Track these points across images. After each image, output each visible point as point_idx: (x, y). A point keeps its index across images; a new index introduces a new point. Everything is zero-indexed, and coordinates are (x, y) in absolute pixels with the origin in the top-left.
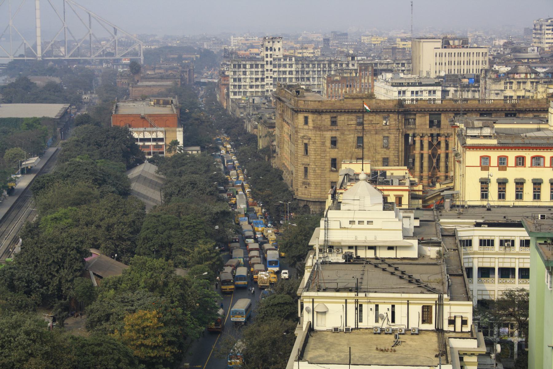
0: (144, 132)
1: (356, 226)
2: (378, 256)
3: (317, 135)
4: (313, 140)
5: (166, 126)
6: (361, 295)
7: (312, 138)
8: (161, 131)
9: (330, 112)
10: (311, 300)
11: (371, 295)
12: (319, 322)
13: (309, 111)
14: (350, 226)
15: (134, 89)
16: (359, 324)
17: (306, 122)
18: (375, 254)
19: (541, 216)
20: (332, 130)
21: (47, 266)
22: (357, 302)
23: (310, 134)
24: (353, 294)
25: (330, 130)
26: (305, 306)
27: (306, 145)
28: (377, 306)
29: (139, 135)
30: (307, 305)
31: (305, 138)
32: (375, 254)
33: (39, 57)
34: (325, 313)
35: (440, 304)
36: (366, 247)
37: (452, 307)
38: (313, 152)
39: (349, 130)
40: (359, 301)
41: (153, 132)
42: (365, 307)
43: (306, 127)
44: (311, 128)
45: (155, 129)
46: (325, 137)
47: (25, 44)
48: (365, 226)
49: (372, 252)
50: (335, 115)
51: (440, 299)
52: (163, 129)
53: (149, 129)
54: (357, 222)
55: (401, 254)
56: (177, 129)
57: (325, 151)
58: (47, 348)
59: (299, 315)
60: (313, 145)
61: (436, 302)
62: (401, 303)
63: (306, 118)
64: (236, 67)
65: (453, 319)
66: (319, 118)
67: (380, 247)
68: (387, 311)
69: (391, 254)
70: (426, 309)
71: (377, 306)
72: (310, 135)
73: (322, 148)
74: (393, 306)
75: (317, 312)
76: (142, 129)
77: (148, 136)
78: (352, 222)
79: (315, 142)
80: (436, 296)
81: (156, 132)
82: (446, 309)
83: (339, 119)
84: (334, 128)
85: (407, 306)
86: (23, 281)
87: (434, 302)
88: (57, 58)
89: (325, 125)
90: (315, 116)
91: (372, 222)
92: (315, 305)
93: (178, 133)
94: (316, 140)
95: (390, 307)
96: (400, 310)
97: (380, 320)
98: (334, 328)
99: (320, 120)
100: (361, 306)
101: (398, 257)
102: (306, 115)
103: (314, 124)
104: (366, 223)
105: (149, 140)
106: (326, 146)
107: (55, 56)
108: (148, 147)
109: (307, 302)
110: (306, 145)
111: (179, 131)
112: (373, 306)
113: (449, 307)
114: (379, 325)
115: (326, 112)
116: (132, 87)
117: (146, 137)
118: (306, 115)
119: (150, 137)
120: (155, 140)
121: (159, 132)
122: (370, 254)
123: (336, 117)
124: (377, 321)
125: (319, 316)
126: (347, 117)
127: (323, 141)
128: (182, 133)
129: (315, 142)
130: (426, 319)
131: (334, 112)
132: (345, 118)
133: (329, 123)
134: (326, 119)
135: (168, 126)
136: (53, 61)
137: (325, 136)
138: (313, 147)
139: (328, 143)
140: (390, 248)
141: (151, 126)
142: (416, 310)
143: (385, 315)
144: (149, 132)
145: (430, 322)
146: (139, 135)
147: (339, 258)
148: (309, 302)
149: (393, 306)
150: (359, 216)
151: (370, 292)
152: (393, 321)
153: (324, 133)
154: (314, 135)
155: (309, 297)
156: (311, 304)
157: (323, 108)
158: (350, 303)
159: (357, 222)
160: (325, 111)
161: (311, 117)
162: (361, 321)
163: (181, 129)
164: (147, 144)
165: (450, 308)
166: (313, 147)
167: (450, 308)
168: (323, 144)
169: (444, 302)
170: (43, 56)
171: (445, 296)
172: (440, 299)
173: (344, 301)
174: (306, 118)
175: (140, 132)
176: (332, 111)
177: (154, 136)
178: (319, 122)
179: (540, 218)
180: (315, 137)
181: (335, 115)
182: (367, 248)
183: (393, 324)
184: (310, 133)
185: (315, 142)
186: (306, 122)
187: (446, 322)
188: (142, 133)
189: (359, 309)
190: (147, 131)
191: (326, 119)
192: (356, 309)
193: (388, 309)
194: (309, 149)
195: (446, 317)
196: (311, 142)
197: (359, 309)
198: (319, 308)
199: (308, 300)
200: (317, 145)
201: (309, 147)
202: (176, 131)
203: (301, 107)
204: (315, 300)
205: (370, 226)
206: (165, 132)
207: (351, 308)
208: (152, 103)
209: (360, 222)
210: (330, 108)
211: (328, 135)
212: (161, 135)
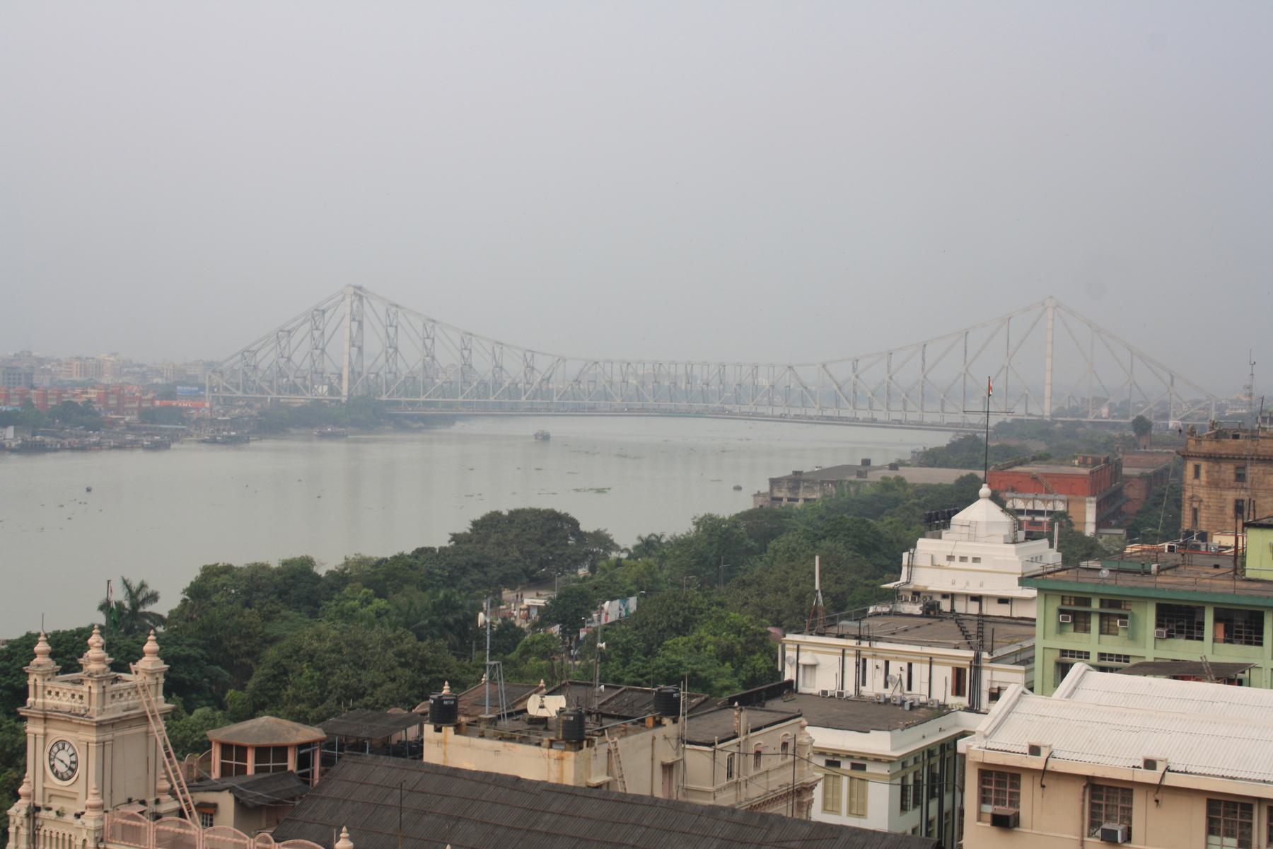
0: (1034, 499)
1: (956, 564)
2: (984, 612)
3: (1211, 496)
4: (1206, 504)
5: (1070, 493)
6: (865, 644)
7: (1204, 500)
8: (1061, 500)
9: (1234, 458)
10: (796, 647)
11: (880, 645)
12: (808, 681)
13: (1200, 457)
14: (946, 563)
15: (1125, 457)
16: (861, 688)
17: (1197, 475)
18: (980, 608)
19: (1169, 547)
20: (1235, 488)
21: (660, 631)
22: (858, 654)
23: (1202, 493)
24: (853, 643)
25: (1233, 488)
26: (788, 654)
27: (1195, 511)
28: (887, 663)
29: (1026, 505)
30: (790, 654)
31: (1195, 499)
32: (980, 608)
33: (1048, 417)
34: (814, 666)
35: (976, 665)
36: (966, 595)
37: (994, 672)
38: (1204, 523)
39: (1266, 490)
40: (862, 653)
41: (1049, 501)
42: (869, 662)
43: (1196, 482)
44: (1203, 483)
45: (1051, 497)
46: (1225, 499)
47: (1027, 395)
48: (969, 565)
49: (977, 604)
50: (1242, 464)
51: (977, 658)
52: (1063, 497)
53: (1043, 496)
54: (957, 559)
55: (1019, 611)
56: (1087, 499)
57: (1224, 522)
58: (426, 679)
59: (780, 669)
60: (1206, 511)
61: (971, 662)
62: (921, 662)
63: (1197, 468)
64: (1266, 422)
65: (996, 691)
66: (1217, 468)
67: (988, 597)
68: (899, 672)
69: (1003, 611)
70: (959, 673)
71: (887, 663)
72: (1201, 495)
73: (1220, 516)
74: (910, 665)
75: (805, 666)
76: (1031, 496)
77: (1040, 506)
78: (950, 558)
79: (1208, 507)
80: (971, 654)
81: (1054, 501)
82: (986, 675)
83: (1249, 471)
84: (1240, 484)
85: (928, 666)
86: (617, 648)
87: (968, 663)
88: (1075, 419)
89: (1224, 480)
90: (1211, 464)
91: (980, 559)
92: (801, 654)
93: (1088, 505)
94: (1211, 504)
95: (905, 666)
96: (920, 671)
97: (890, 685)
98: (823, 691)
99: (1218, 472)
100: (865, 660)
101: (1015, 615)
102: (1197, 462)
103: (1208, 478)
104: (970, 560)
105: (1041, 513)
106: (1226, 514)
107: (1072, 417)
108: (1040, 523)
109: (790, 649)
110: (1195, 511)
111: (1091, 502)
112: (881, 663)
113: (989, 672)
114: (888, 693)
115: (1226, 458)
116: (1123, 454)
117: (1036, 508)
118: (1197, 462)
119: (1042, 508)
120: (1050, 513)
121: (1057, 502)
122: (973, 608)
123: (1244, 468)
124: (886, 686)
125: (808, 671)
126: (1263, 468)
127: (1222, 505)
128: (1094, 505)
129: (1209, 506)
130: (958, 691)
131: (1239, 459)
132: (1259, 470)
133: (1232, 477)
134: (1228, 471)
135: (1075, 494)
136: (1062, 422)
137: (1224, 497)
138: (1204, 515)
139: (1230, 510)
140: (1003, 601)
141: (1047, 492)
142: (944, 674)
143: (898, 677)
144: (1043, 500)
145: (964, 695)
146: (1026, 505)
147: (916, 609)
148: (793, 649)
149: (910, 665)
150: (969, 549)
151: (878, 639)
152: (909, 688)
153: (1225, 492)
154: (1206, 496)
155: (793, 642)
156: (795, 653)
157: (1223, 452)
158: (849, 655)
159: (957, 559)
160: (1225, 456)
161: (1204, 466)
162: (864, 684)
163: (1094, 499)
164: (1038, 519)
165: (992, 674)
166: (1204, 515)
167: (992, 674)
168: (1221, 510)
169: (984, 664)
170: (1052, 415)
171: (985, 655)
172: (977, 658)
173: (841, 651)
174: (1197, 468)
175: (1029, 500)
176: (1237, 457)
177: (1050, 507)
178: (1216, 474)
179: (1166, 551)
180: (1209, 498)
181: (1242, 464)
182: (969, 599)
183: (909, 692)
184: (1201, 491)
185: (1208, 507)
186: (1197, 475)
187: (985, 697)
188: (1031, 502)
189: (861, 666)
190: (1039, 499)
191: (1228, 471)
192: (857, 665)
193: (901, 669)
194: (1199, 518)
195: (985, 687)
196: (1202, 507)
197: (861, 666)
198: (805, 659)
199: (791, 646)
200: (1211, 511)
201: (1199, 514)
202: (1084, 502)
203: (1191, 449)
204: (801, 647)
205: (976, 566)
206: (1068, 503)
207: (851, 662)
208: (1076, 462)
209: (963, 559)
210: (1235, 452)
211: (1231, 496)
212: (1060, 507)
